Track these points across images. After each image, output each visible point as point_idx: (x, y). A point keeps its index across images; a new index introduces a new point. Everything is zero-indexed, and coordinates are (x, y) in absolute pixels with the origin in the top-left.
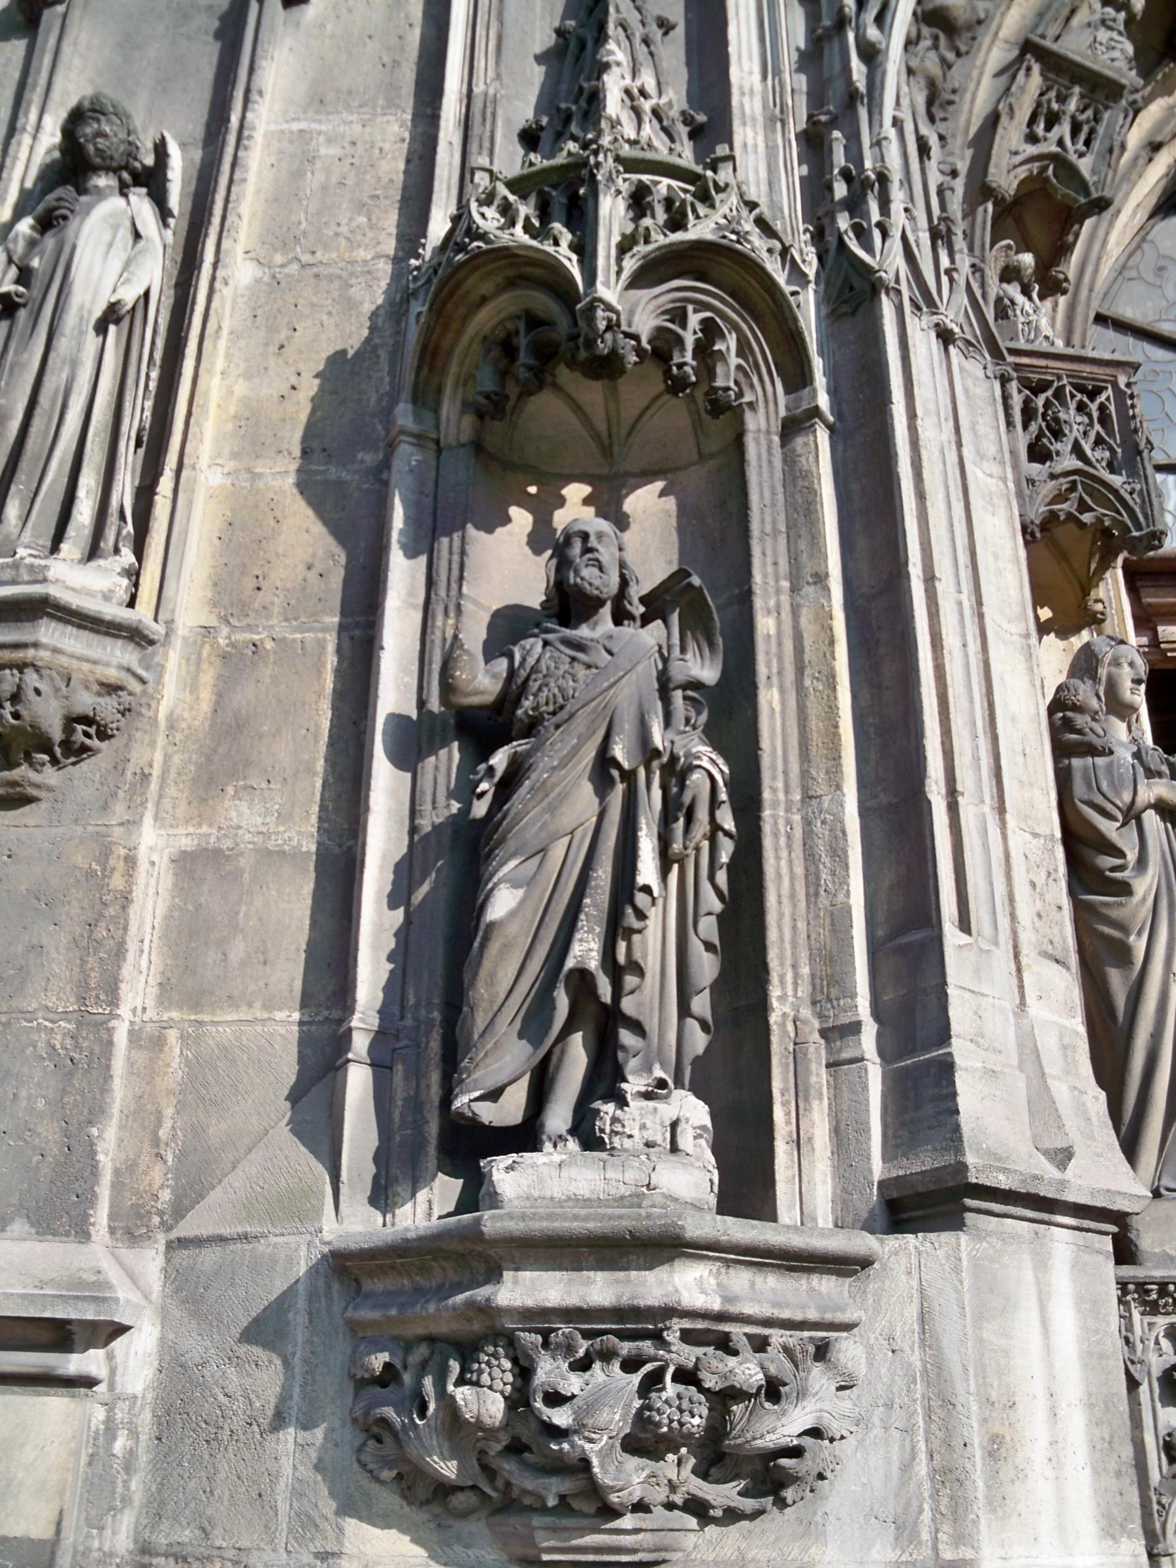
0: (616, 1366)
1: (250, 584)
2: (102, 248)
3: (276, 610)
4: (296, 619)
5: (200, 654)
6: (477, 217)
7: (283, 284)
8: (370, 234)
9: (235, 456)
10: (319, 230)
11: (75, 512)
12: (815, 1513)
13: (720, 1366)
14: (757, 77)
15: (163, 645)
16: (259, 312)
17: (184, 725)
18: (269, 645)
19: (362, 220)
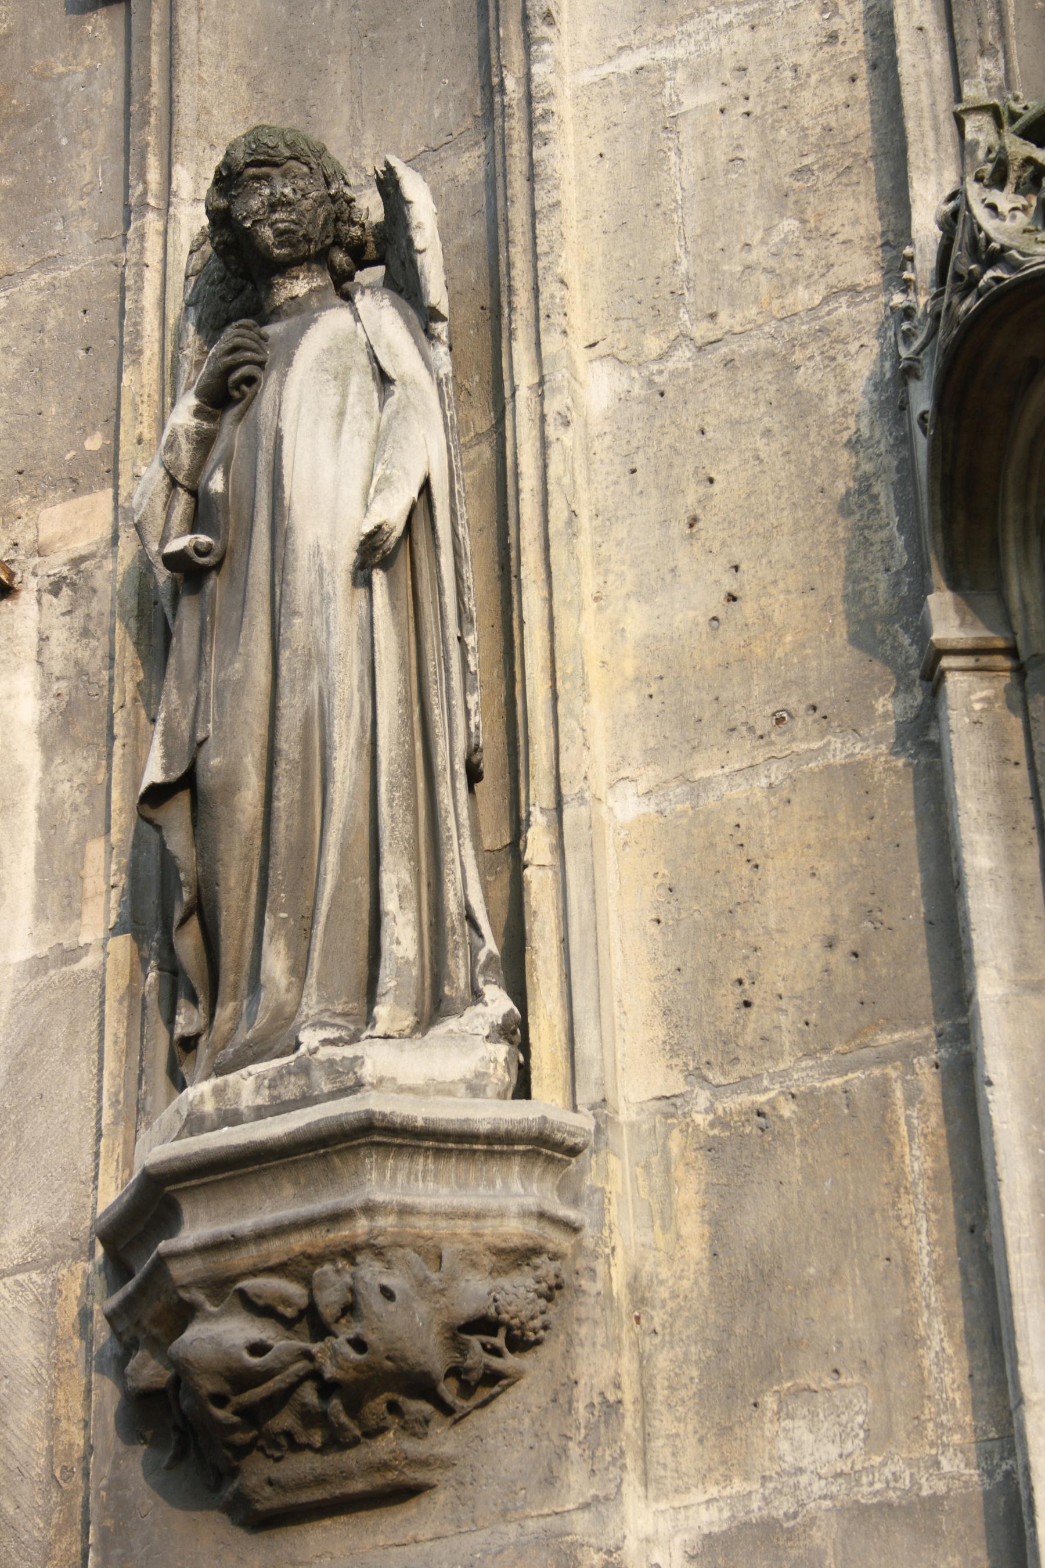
1: (731, 998)
2: (327, 426)
3: (786, 1039)
4: (825, 1049)
5: (665, 1151)
6: (981, 214)
7: (670, 394)
8: (810, 253)
9: (653, 755)
10: (714, 269)
11: (386, 941)
15: (596, 1151)
16: (639, 461)
17: (663, 1293)
18: (787, 1110)
19: (789, 225)
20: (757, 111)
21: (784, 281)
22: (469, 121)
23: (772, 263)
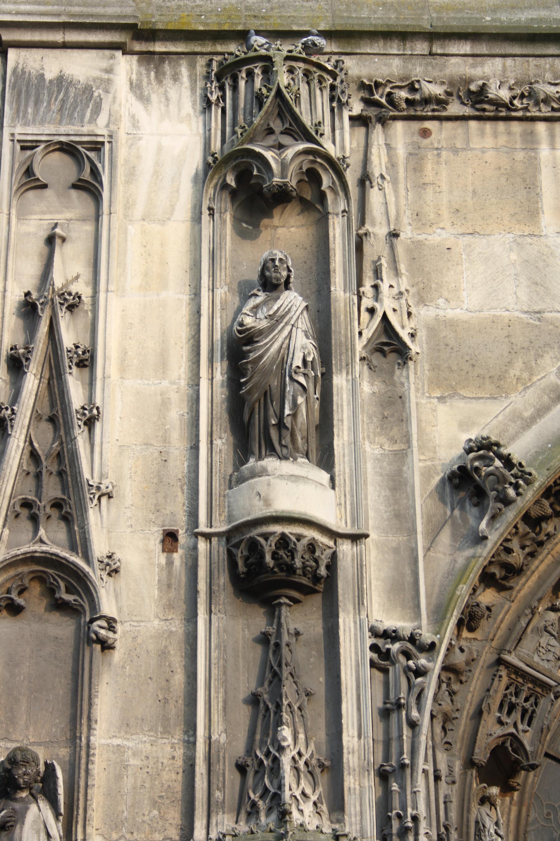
8: (161, 823)
10: (134, 819)
14: (356, 739)
19: (155, 812)
20: (150, 773)
21: (153, 830)
22: (64, 738)
23: (150, 822)
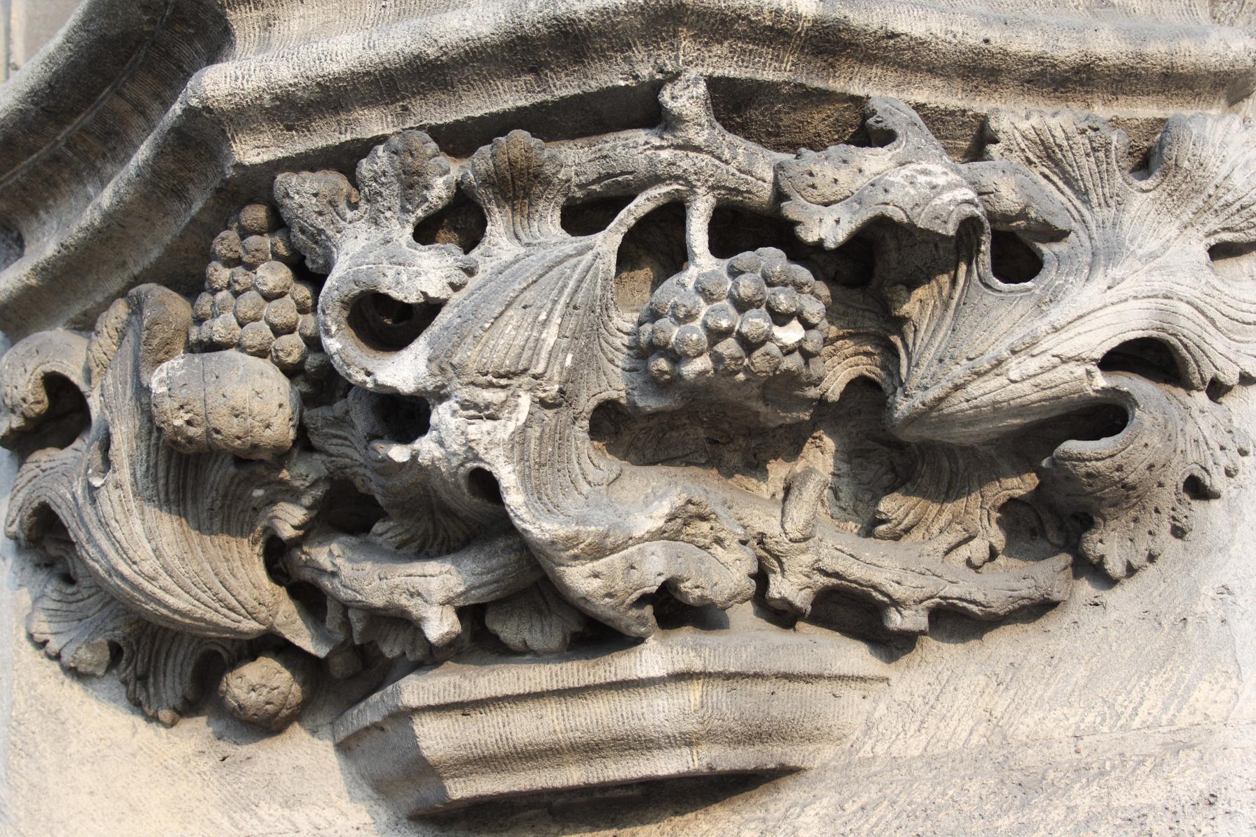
0: (549, 225)
12: (1194, 593)
13: (844, 175)
